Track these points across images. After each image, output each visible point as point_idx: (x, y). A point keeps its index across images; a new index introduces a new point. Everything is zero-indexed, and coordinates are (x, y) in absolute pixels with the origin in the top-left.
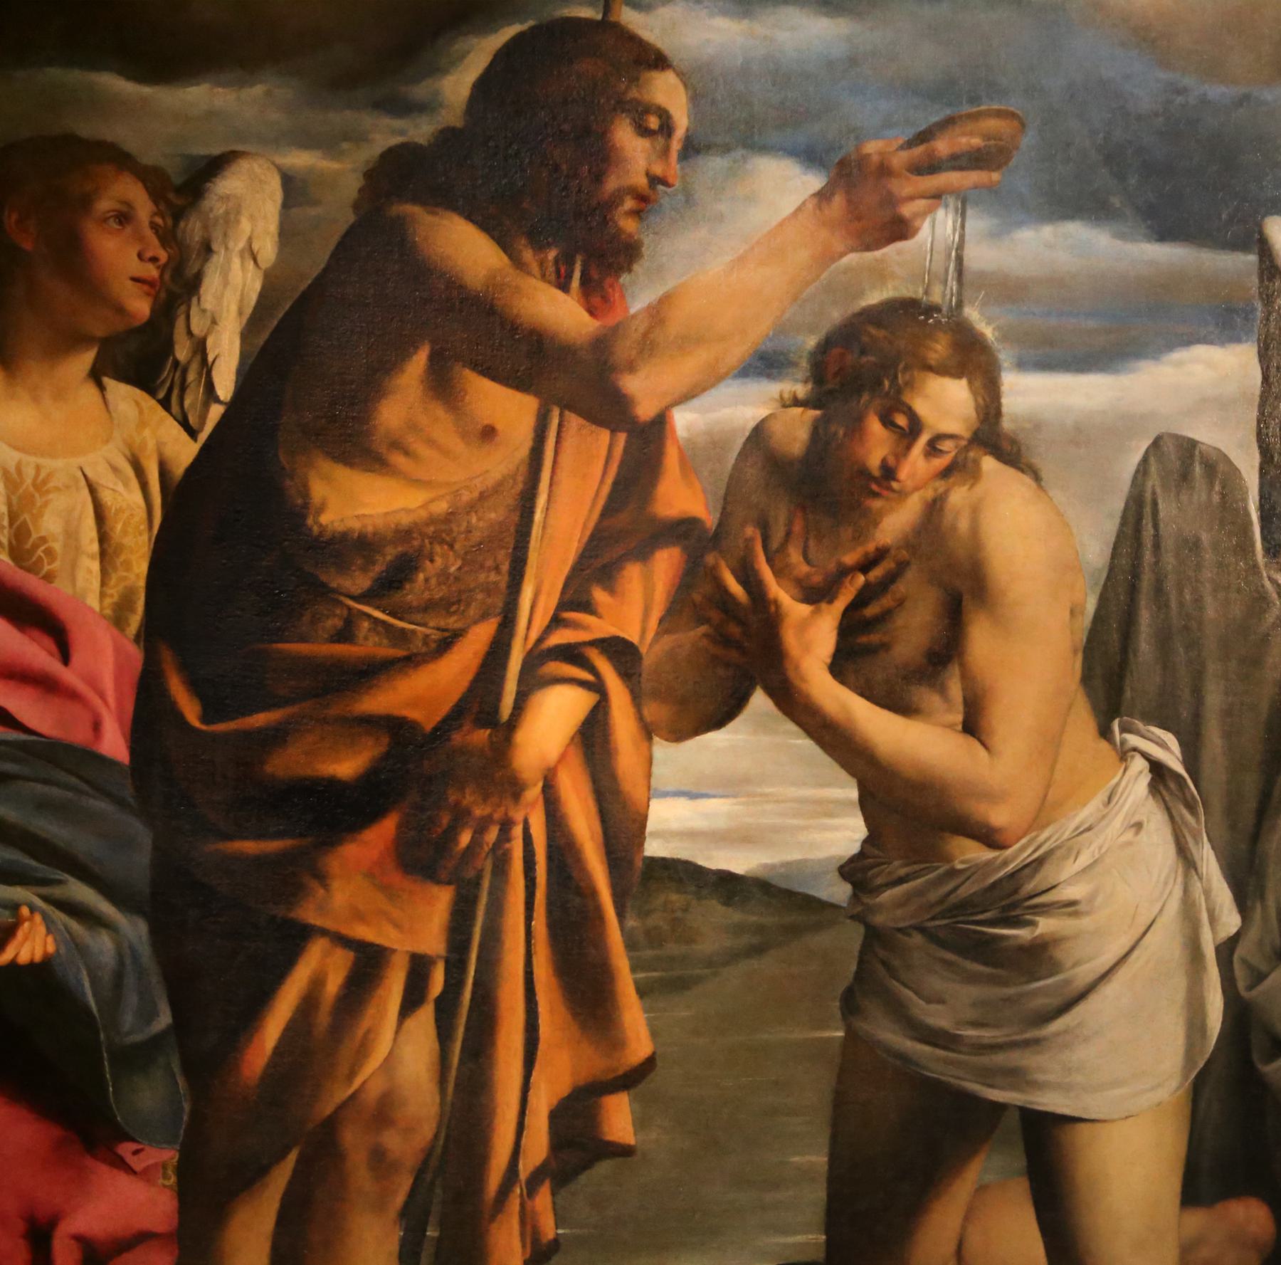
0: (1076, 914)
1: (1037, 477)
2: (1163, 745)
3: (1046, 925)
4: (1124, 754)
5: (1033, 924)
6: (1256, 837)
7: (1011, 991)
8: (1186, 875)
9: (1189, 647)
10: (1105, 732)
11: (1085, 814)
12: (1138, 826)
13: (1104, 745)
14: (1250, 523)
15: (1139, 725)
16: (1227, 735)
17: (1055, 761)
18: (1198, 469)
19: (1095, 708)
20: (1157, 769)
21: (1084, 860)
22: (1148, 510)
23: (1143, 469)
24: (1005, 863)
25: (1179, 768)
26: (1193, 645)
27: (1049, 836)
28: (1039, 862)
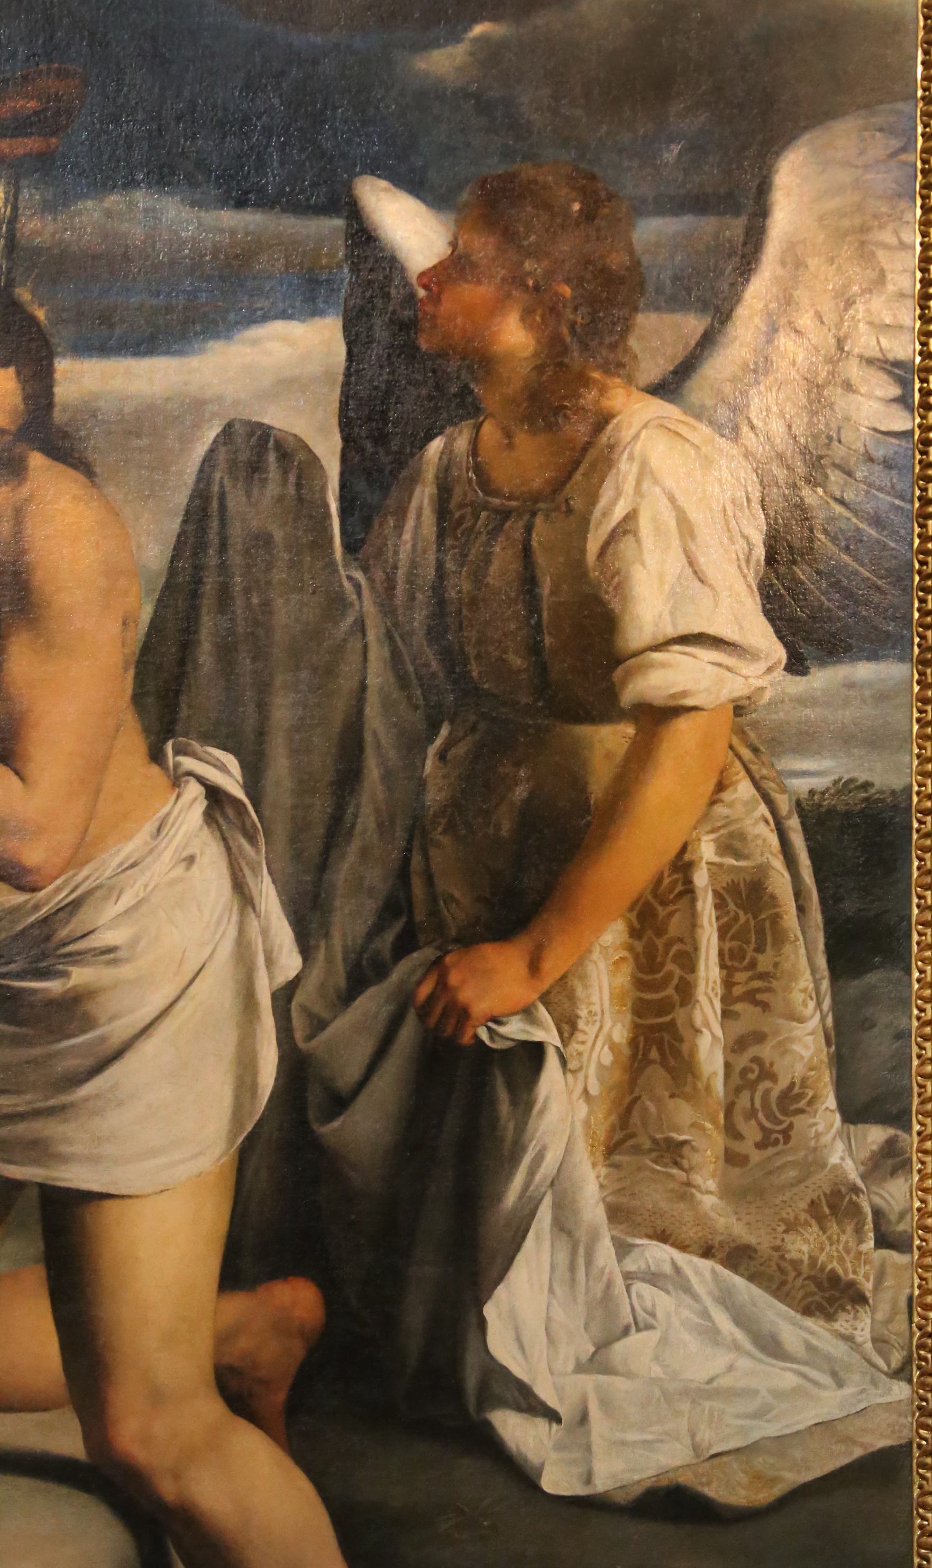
0: (115, 962)
1: (85, 468)
2: (223, 768)
3: (79, 976)
4: (177, 779)
5: (65, 975)
6: (323, 866)
7: (37, 1051)
8: (242, 913)
9: (254, 659)
10: (156, 756)
11: (130, 848)
12: (191, 860)
13: (155, 769)
14: (328, 515)
15: (196, 745)
16: (294, 752)
17: (98, 792)
18: (272, 457)
19: (147, 730)
20: (214, 795)
21: (127, 900)
22: (215, 504)
23: (209, 459)
24: (37, 907)
25: (239, 793)
26: (260, 654)
27: (86, 876)
28: (74, 906)
